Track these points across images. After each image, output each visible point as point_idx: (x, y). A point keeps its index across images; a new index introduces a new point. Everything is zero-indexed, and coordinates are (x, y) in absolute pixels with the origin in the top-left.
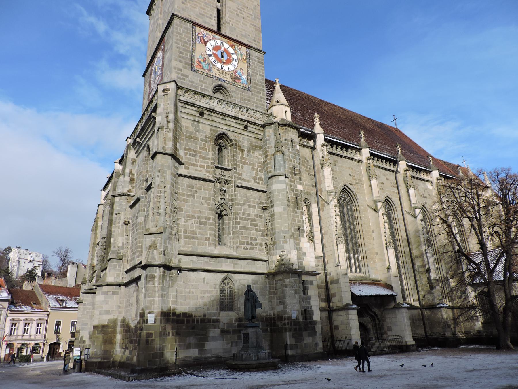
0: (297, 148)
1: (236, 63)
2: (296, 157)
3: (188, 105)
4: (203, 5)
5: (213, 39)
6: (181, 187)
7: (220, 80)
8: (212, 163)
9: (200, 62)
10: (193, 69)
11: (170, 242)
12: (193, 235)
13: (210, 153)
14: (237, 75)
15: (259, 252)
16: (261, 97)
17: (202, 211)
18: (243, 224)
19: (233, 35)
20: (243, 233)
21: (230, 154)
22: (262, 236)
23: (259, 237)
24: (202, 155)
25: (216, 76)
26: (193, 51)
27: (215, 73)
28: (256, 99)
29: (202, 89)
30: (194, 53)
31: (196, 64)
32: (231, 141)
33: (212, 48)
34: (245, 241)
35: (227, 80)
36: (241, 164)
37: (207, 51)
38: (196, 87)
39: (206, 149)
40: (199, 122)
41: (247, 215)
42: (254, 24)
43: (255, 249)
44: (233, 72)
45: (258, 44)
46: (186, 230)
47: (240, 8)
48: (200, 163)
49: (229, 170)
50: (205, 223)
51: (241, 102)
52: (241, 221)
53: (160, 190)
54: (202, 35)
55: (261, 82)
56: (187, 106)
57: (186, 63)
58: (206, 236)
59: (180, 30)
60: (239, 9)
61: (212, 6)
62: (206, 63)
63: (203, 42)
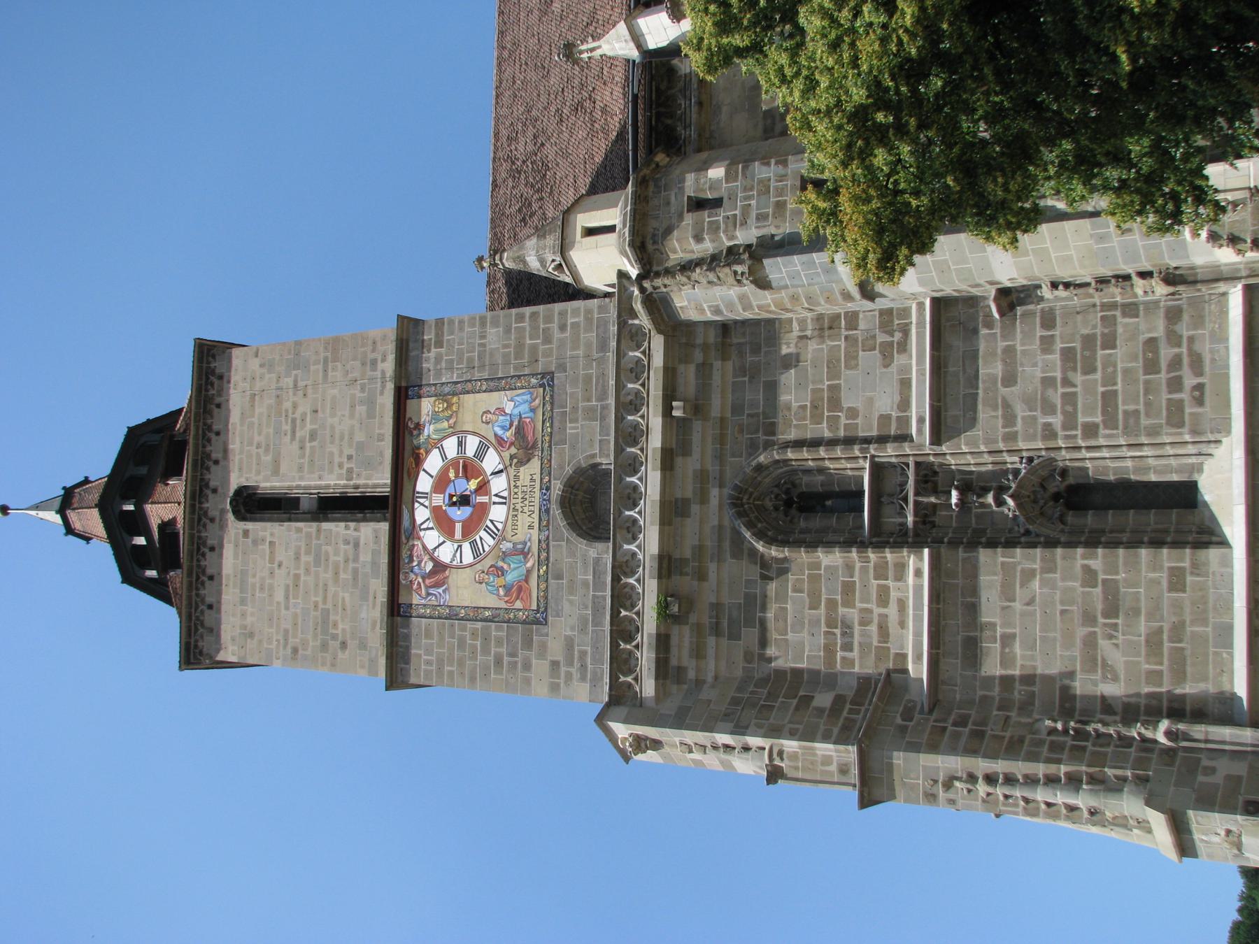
0: (719, 181)
1: (472, 444)
2: (761, 181)
6: (980, 693)
7: (547, 511)
9: (508, 589)
10: (539, 619)
11: (1205, 762)
12: (1167, 645)
14: (508, 435)
15: (1209, 326)
16: (563, 328)
17: (1062, 603)
18: (1090, 410)
19: (381, 454)
20: (1131, 407)
22: (1131, 309)
23: (1142, 327)
24: (839, 597)
25: (536, 525)
26: (475, 615)
27: (527, 529)
28: (573, 349)
29: (598, 584)
31: (518, 604)
33: (448, 543)
34: (1165, 396)
35: (537, 477)
36: (843, 421)
38: (597, 610)
39: (814, 579)
41: (1050, 392)
43: (1197, 347)
44: (506, 455)
45: (380, 348)
46: (1150, 673)
47: (288, 428)
48: (872, 606)
49: (878, 470)
50: (1111, 591)
51: (603, 418)
52: (1081, 419)
53: (1001, 798)
54: (420, 580)
55: (508, 330)
56: (674, 662)
57: (528, 643)
58: (1165, 584)
59: (428, 663)
60: (294, 432)
61: (318, 538)
62: (505, 567)
63: (441, 576)
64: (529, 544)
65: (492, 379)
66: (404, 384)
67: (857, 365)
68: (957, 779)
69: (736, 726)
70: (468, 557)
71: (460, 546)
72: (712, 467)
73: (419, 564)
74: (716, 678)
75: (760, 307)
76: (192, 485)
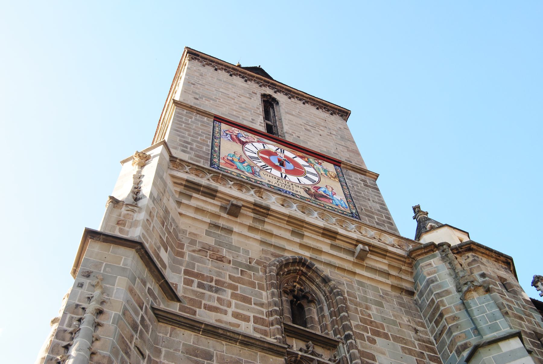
3: (198, 191)
4: (236, 108)
5: (258, 142)
6: (163, 350)
8: (270, 314)
13: (264, 293)
14: (321, 191)
21: (326, 312)
25: (271, 183)
30: (216, 149)
32: (326, 280)
36: (365, 334)
37: (246, 152)
40: (230, 231)
42: (344, 145)
44: (310, 187)
47: (310, 124)
48: (233, 309)
54: (235, 134)
55: (379, 211)
56: (195, 195)
61: (254, 112)
63: (237, 141)
64: (259, 177)
65: (351, 196)
66: (342, 165)
67: (406, 353)
68: (103, 293)
69: (154, 197)
70: (248, 154)
71: (255, 153)
72: (323, 258)
73: (243, 136)
74: (180, 214)
75: (442, 301)
76: (278, 86)
